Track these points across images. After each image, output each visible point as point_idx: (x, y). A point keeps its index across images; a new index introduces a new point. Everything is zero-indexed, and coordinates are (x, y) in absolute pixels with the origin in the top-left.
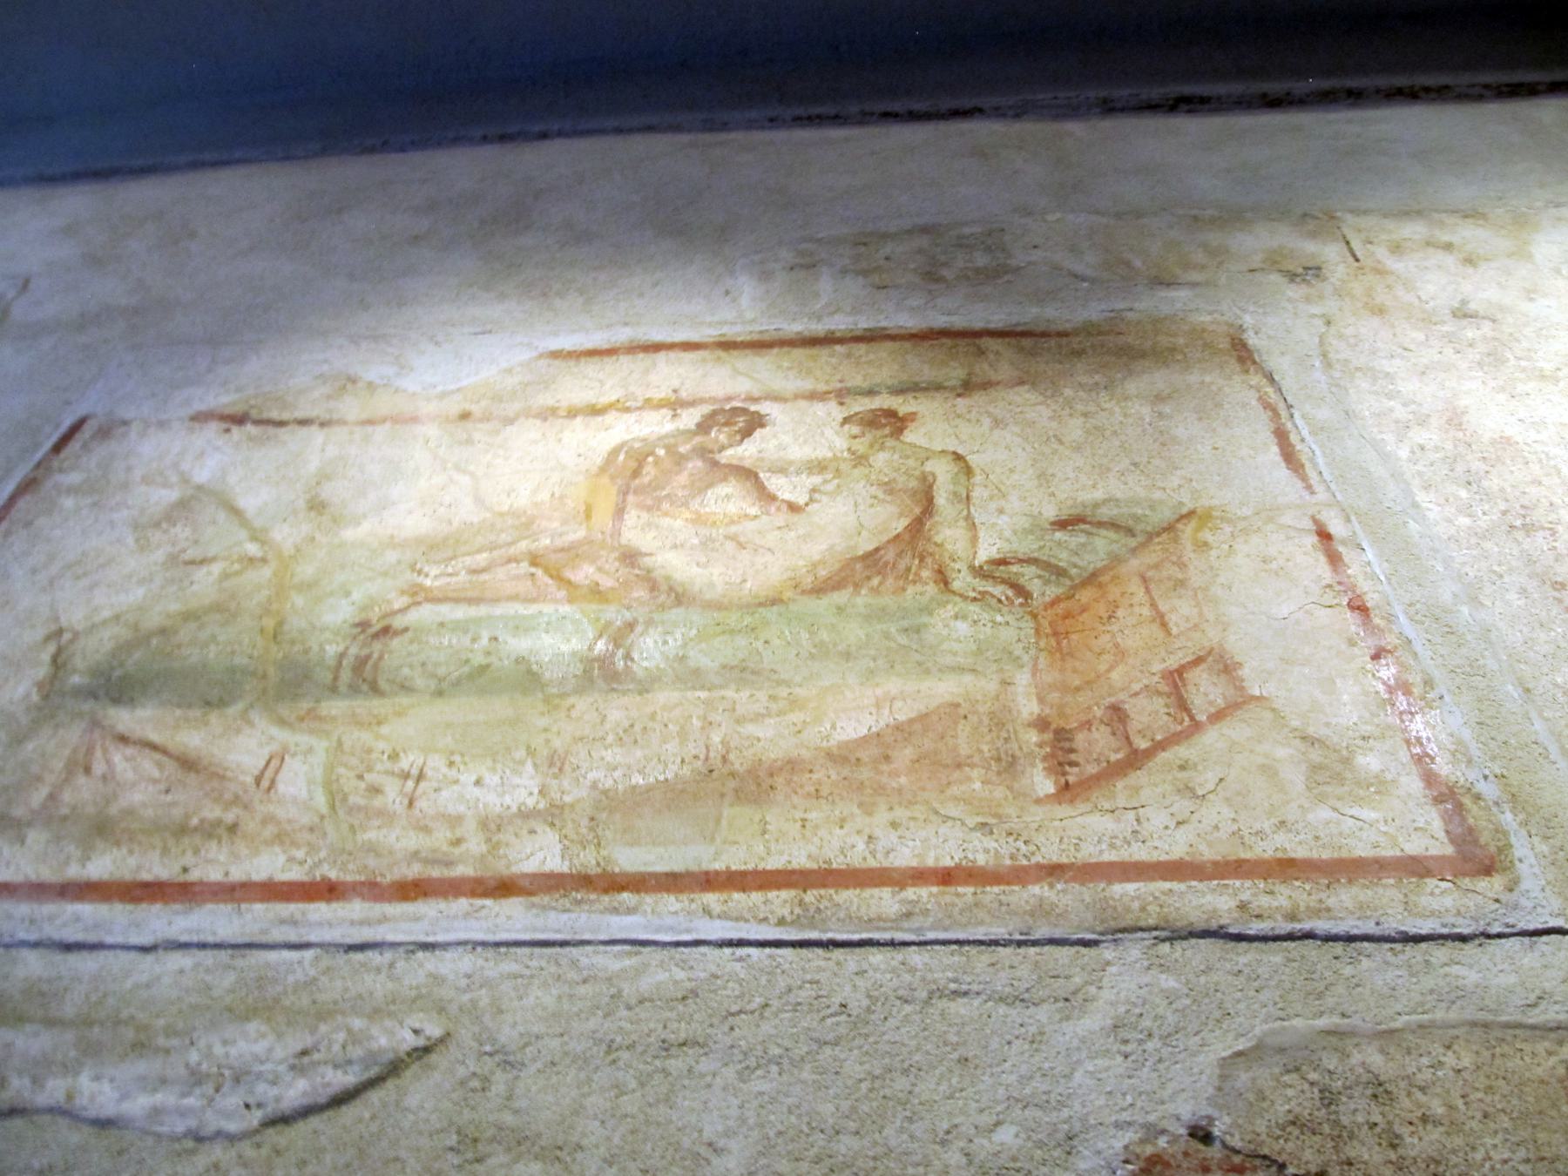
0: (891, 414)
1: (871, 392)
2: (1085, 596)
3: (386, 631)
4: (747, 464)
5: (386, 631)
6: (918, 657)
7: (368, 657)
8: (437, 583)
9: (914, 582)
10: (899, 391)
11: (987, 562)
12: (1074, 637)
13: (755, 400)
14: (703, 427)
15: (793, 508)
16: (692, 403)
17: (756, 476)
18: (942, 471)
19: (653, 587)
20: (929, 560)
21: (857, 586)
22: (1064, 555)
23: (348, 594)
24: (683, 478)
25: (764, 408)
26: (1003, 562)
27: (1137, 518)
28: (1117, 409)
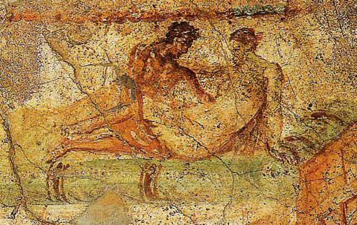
0: (251, 32)
1: (243, 15)
2: (320, 159)
3: (60, 166)
4: (191, 67)
5: (60, 166)
6: (257, 191)
7: (58, 181)
8: (74, 139)
9: (257, 149)
10: (256, 15)
11: (286, 138)
12: (312, 183)
13: (191, 17)
14: (169, 39)
15: (211, 100)
16: (163, 18)
17: (194, 74)
18: (271, 74)
19: (160, 147)
20: (263, 136)
21: (236, 149)
22: (314, 136)
23: (39, 144)
24: (164, 76)
25: (195, 23)
26: (291, 139)
27: (345, 114)
28: (350, 35)
